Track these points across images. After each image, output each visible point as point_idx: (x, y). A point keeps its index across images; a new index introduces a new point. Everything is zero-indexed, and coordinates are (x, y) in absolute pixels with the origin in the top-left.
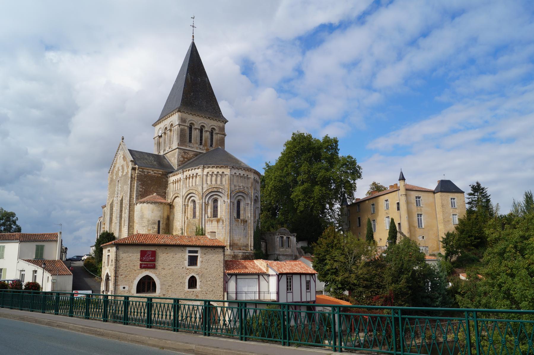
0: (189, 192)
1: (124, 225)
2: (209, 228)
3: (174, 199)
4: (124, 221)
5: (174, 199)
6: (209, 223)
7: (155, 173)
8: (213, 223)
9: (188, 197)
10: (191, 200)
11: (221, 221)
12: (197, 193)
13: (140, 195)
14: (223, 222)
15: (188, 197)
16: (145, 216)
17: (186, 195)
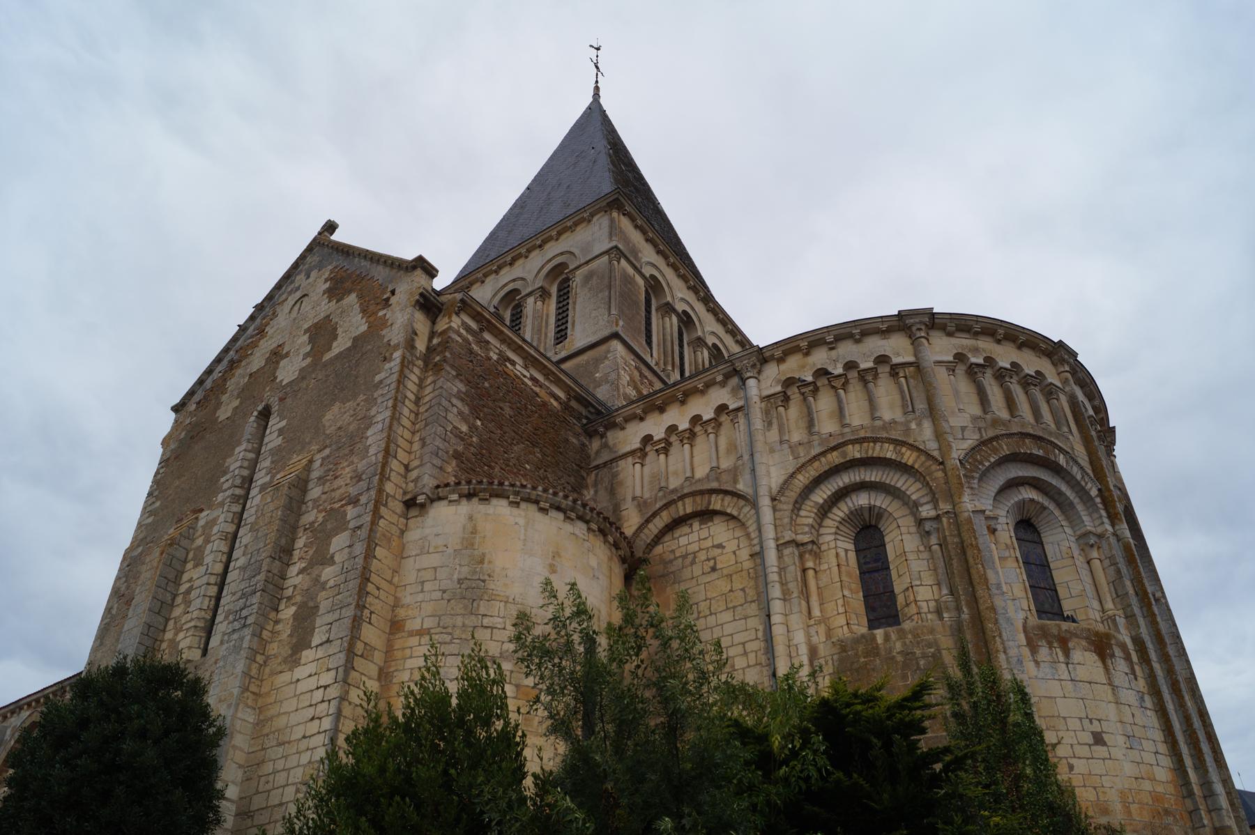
0: (835, 458)
1: (301, 642)
2: (1055, 689)
3: (658, 539)
4: (306, 616)
5: (658, 539)
6: (1044, 652)
7: (533, 379)
8: (1077, 655)
9: (820, 496)
10: (840, 512)
11: (1118, 652)
12: (909, 457)
13: (457, 455)
14: (1128, 658)
15: (820, 496)
16: (495, 586)
17: (802, 480)
